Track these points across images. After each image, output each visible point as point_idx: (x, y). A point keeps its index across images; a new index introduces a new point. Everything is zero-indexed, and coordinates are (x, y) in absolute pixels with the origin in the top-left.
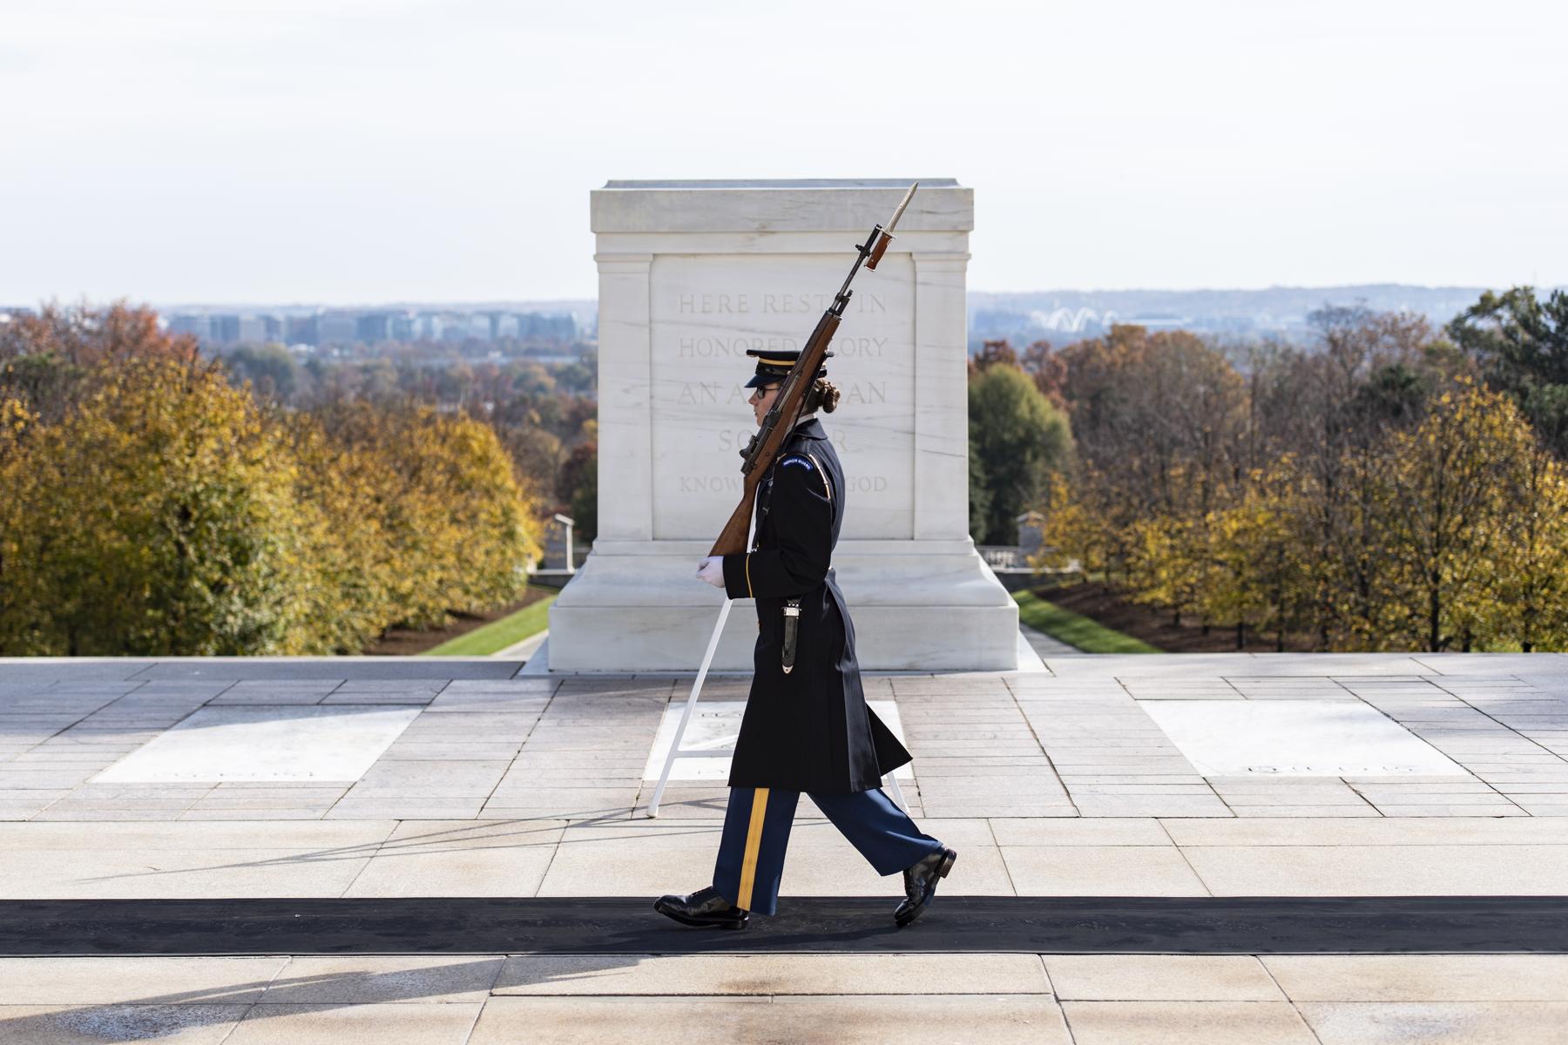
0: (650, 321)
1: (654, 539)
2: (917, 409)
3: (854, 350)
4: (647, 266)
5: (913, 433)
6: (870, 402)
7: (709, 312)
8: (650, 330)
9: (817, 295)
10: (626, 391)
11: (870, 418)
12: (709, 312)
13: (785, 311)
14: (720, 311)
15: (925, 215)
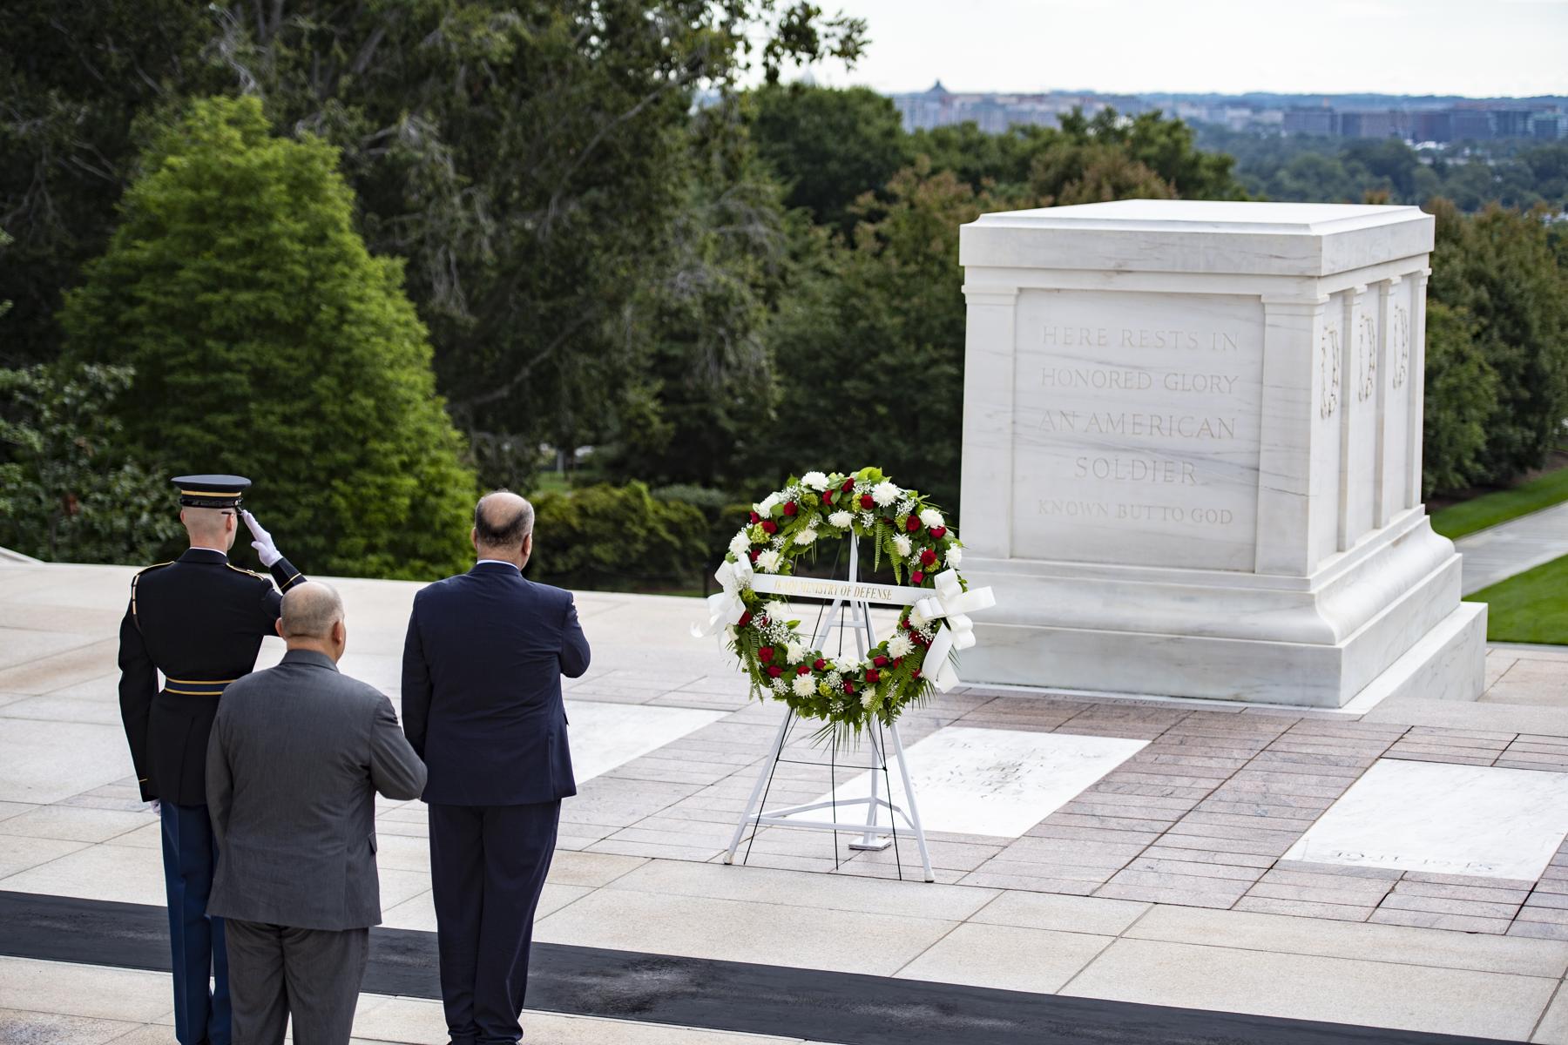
0: (1015, 350)
1: (1011, 557)
2: (1263, 447)
3: (1206, 387)
4: (1012, 300)
5: (1258, 470)
6: (1220, 437)
7: (1070, 344)
8: (1015, 359)
9: (1171, 332)
10: (989, 416)
11: (1218, 453)
12: (1070, 344)
13: (1141, 346)
14: (1081, 344)
15: (1274, 260)
